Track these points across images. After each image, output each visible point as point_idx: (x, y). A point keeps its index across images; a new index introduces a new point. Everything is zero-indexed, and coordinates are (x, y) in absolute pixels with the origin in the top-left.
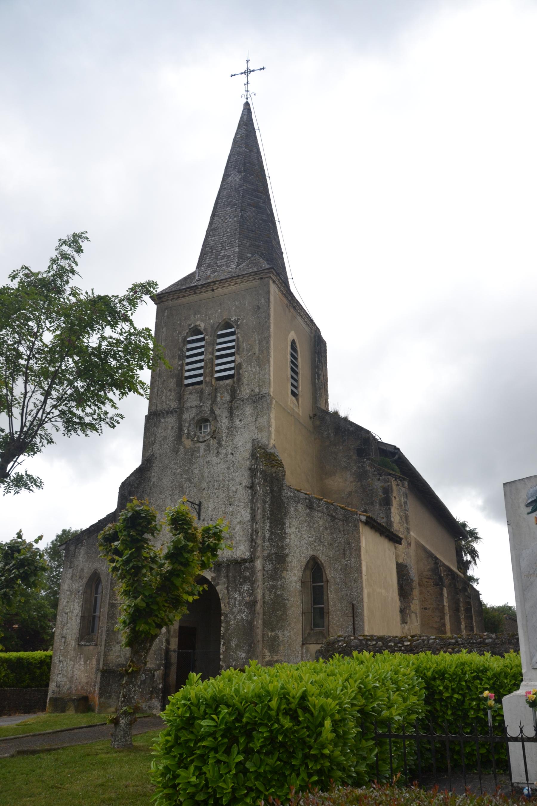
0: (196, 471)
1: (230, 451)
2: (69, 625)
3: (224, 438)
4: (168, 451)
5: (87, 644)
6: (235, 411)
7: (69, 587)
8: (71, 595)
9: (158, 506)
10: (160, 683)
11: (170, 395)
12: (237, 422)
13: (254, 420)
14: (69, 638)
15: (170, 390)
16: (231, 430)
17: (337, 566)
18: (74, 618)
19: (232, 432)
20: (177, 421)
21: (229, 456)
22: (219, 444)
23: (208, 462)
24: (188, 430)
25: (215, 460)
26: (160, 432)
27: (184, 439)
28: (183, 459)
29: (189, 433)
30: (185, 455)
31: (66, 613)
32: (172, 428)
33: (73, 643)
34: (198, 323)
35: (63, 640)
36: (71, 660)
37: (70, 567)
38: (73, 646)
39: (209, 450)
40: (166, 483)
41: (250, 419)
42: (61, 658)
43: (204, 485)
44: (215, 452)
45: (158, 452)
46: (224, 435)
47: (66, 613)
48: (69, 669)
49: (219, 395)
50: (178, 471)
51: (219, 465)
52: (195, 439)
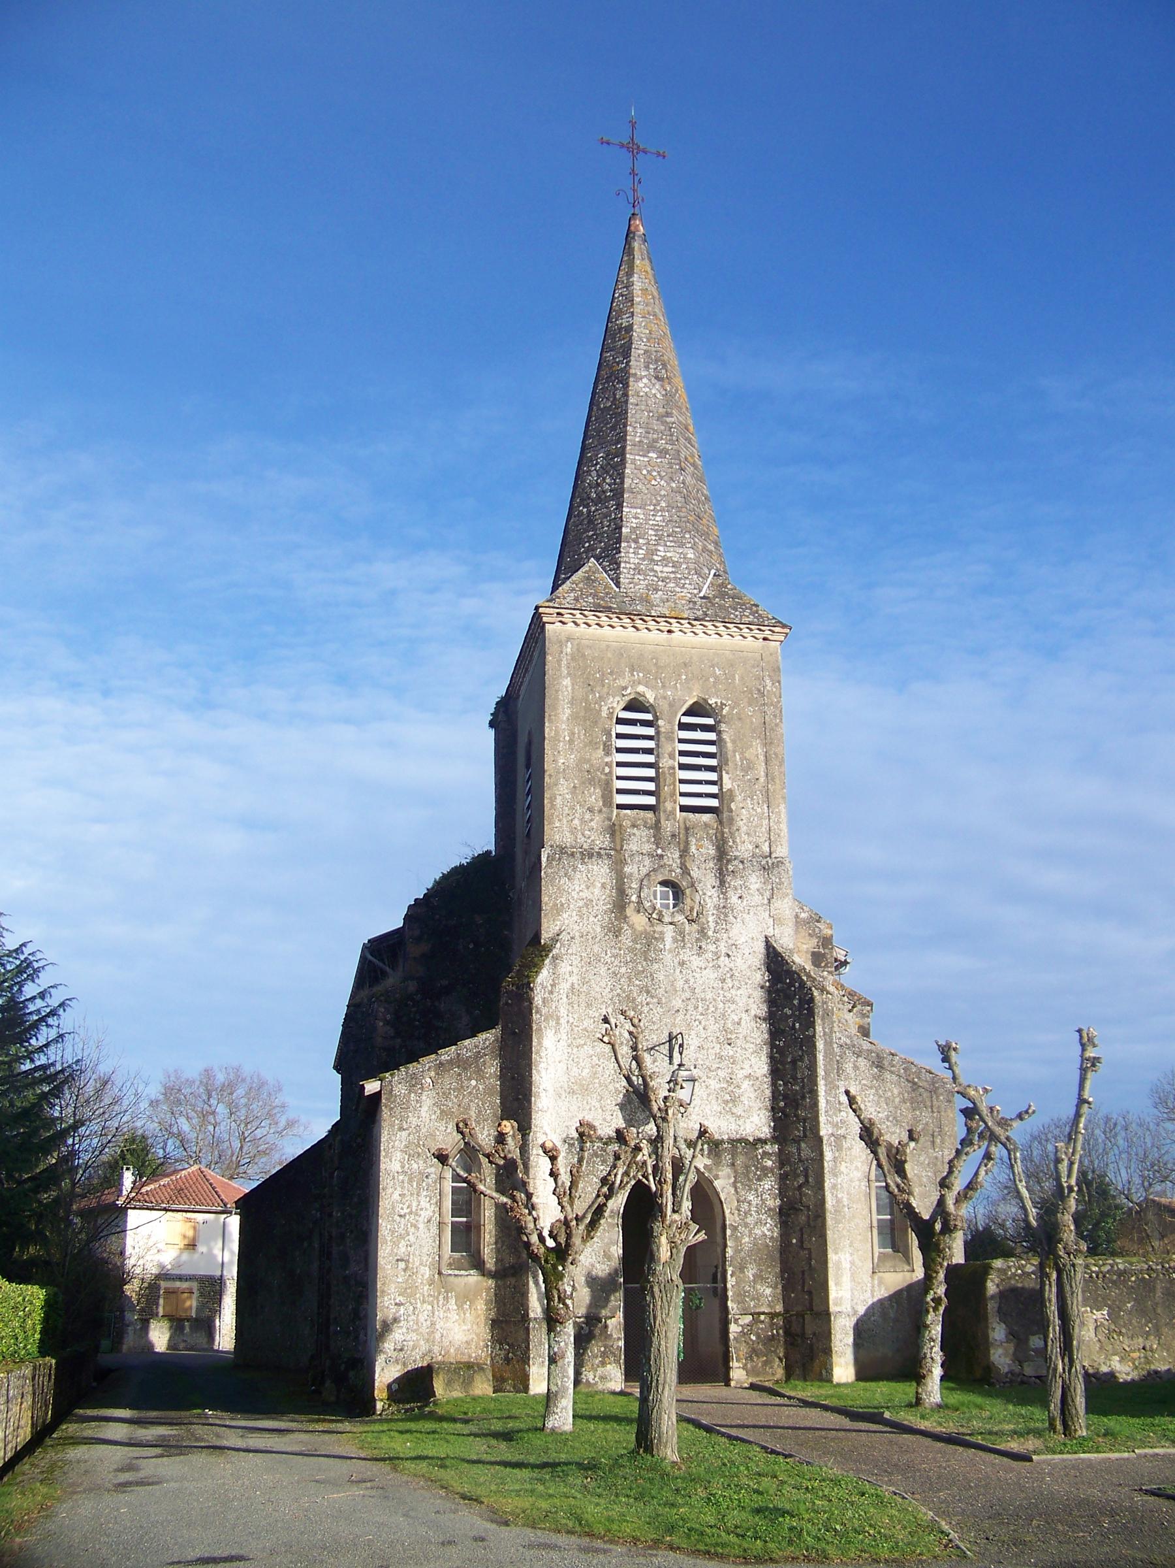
0: (661, 976)
1: (724, 950)
2: (412, 1238)
3: (712, 925)
4: (598, 929)
5: (463, 1272)
6: (729, 879)
7: (403, 1167)
8: (410, 1180)
9: (585, 1030)
10: (619, 1339)
11: (592, 820)
12: (734, 899)
13: (766, 901)
14: (415, 1261)
15: (591, 810)
16: (724, 911)
17: (922, 1158)
18: (421, 1226)
19: (726, 916)
20: (614, 876)
21: (722, 958)
22: (702, 932)
23: (682, 964)
24: (639, 897)
25: (696, 962)
26: (577, 888)
27: (630, 911)
28: (631, 950)
29: (640, 902)
30: (635, 941)
31: (400, 1216)
32: (603, 886)
33: (426, 1272)
34: (641, 689)
35: (402, 1265)
36: (424, 1302)
37: (401, 1129)
38: (427, 1276)
39: (683, 941)
40: (598, 989)
41: (757, 899)
42: (400, 1299)
43: (677, 1003)
44: (695, 948)
45: (576, 927)
46: (711, 919)
47: (400, 1216)
48: (422, 1318)
49: (693, 841)
50: (623, 970)
51: (704, 972)
52: (654, 916)
